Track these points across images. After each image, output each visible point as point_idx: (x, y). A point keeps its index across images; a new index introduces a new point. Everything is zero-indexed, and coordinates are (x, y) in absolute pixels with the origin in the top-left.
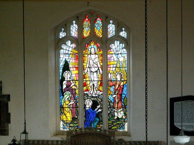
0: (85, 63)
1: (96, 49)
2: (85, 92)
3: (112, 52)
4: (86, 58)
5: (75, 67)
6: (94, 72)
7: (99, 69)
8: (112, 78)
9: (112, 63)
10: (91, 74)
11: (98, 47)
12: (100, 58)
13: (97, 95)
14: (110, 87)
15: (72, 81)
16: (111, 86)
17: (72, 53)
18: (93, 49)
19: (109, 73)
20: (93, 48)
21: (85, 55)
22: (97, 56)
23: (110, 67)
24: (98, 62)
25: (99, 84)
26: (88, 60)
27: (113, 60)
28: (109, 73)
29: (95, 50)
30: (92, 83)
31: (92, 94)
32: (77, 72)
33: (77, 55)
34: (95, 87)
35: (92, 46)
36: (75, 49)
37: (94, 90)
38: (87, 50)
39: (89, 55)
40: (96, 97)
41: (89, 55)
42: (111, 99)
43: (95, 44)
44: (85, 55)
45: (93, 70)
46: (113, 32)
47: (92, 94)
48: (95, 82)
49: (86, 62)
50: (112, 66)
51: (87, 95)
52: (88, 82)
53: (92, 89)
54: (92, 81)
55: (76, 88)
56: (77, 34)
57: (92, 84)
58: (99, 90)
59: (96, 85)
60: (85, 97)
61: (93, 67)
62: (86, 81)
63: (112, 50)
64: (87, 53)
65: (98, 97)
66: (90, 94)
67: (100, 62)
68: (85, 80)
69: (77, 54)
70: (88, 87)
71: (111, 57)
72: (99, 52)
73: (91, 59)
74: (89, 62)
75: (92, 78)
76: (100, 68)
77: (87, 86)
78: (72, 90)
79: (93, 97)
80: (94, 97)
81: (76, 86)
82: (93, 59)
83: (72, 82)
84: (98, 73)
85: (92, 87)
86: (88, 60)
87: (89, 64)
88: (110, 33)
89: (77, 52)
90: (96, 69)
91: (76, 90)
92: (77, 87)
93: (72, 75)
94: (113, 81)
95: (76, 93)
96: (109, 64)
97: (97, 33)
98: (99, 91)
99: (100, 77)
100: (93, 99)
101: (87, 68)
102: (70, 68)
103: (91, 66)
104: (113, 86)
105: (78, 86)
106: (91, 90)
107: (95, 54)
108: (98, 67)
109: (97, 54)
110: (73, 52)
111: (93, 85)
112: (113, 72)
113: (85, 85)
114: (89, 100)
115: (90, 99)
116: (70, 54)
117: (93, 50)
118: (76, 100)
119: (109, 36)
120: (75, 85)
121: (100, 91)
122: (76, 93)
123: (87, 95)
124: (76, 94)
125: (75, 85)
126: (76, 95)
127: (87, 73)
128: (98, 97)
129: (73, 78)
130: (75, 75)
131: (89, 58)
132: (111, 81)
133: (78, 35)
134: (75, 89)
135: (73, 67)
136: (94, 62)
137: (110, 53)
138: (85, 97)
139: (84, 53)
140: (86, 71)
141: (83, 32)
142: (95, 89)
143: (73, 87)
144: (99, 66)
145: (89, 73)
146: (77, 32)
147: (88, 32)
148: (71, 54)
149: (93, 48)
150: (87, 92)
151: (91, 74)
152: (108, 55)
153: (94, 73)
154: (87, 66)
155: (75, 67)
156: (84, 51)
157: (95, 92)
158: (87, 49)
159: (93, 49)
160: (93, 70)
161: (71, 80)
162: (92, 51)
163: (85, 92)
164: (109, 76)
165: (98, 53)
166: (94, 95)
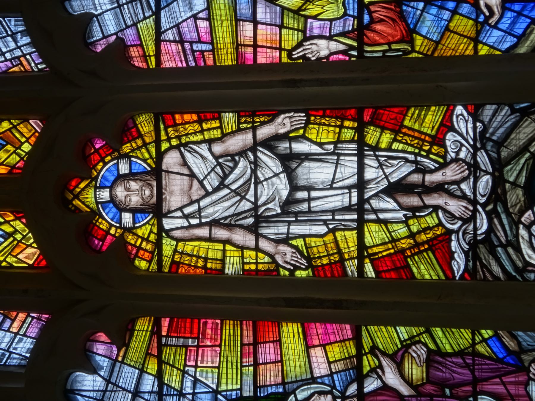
0: (223, 261)
1: (124, 168)
2: (459, 263)
3: (147, 28)
4: (189, 247)
5: (255, 344)
6: (294, 188)
7: (269, 144)
8: (338, 28)
9: (223, 34)
10: (304, 207)
11: (114, 150)
12: (190, 128)
13: (482, 158)
14: (411, 42)
15: (360, 378)
16: (409, 35)
17: (152, 366)
18: (120, 192)
19: (296, 54)
20: (110, 195)
21: (167, 262)
22: (171, 160)
23: (255, 46)
24: (218, 148)
25: (386, 138)
26: (204, 232)
27: (203, 25)
28: (296, 54)
29: (131, 176)
30: (375, 204)
31: (474, 202)
32: (291, 332)
33: (165, 323)
34: (416, 178)
35: (105, 195)
36: (122, 338)
37: (440, 188)
38: (130, 239)
39: (167, 224)
40: (499, 166)
41: (167, 224)
42: (520, 28)
43: (85, 170)
44: (167, 262)
45: (275, 187)
46: (13, 35)
47: (474, 202)
48: (369, 174)
49: (214, 251)
50: (247, 29)
51: (482, 251)
52: (368, 241)
53: (431, 200)
54: (362, 201)
55: (422, 352)
56: (22, 316)
57: (389, 204)
58: (438, 140)
59: (400, 171)
60: (496, 269)
61: (250, 196)
62: (361, 258)
63: (130, 35)
64: (153, 237)
65: (499, 144)
66: (473, 218)
67: (217, 133)
68: (351, 267)
69: (157, 325)
70: (412, 235)
71: (182, 41)
72: (145, 145)
73: (195, 207)
74: (215, 223)
75: (337, 200)
76: (264, 132)
77: (404, 244)
78: (442, 384)
79: (497, 195)
80: (499, 181)
81: (406, 346)
82: (196, 192)
83: (371, 385)
84: (300, 147)
85: (414, 201)
86: (204, 232)
87: (229, 227)
88: (18, 53)
89: (143, 326)
90: (270, 164)
91: (439, 352)
92: (413, 341)
93: (313, 380)
94: (366, 18)
95: (461, 353)
96: (227, 59)
97: (14, 159)
98: (450, 137)
99: (327, 135)
100: (515, 197)
101: (264, 244)
102: (262, 394)
103: (246, 205)
104: (402, 17)
105: (404, 332)
106: (436, 208)
107: (157, 172)
108: (253, 149)
109: (160, 156)
110: (148, 354)
111: (394, 190)
112: (289, 21)
113: (395, 264)
114: (523, 232)
115: (515, 223)
116: (161, 384)
117: (134, 194)
118: (523, 350)
119: (35, 63)
120: (398, 359)
121: (447, 125)
122: (467, 354)
123: (482, 251)
124: (476, 354)
125: (392, 357)
126: (481, 349)
127: (299, 242)
128: (499, 144)
129: (340, 366)
130: (317, 353)
131: (183, 223)
132: (360, 33)
133: (28, 311)
134: (434, 357)
135: (256, 364)
136: (213, 181)
137: (151, 50)
138: (496, 269)
139: (154, 266)
140: (286, 255)
141: (11, 266)
142: (430, 178)
143: (416, 372)
144: (247, 138)
145: (295, 229)
146: (14, 314)
147: (9, 229)
148: (159, 375)
149: (110, 195)
150: (454, 245)
151: (304, 207)
152: (168, 63)
153: (302, 183)
154: (249, 240)
155: (255, 344)
156: (143, 265)
157: (450, 173)
158: (121, 241)
159: (120, 192)
160: (275, 187)
161: (353, 389)
162: (135, 200)
163: (459, 263)
164: (322, 48)
165: (152, 149)
166: (485, 182)
